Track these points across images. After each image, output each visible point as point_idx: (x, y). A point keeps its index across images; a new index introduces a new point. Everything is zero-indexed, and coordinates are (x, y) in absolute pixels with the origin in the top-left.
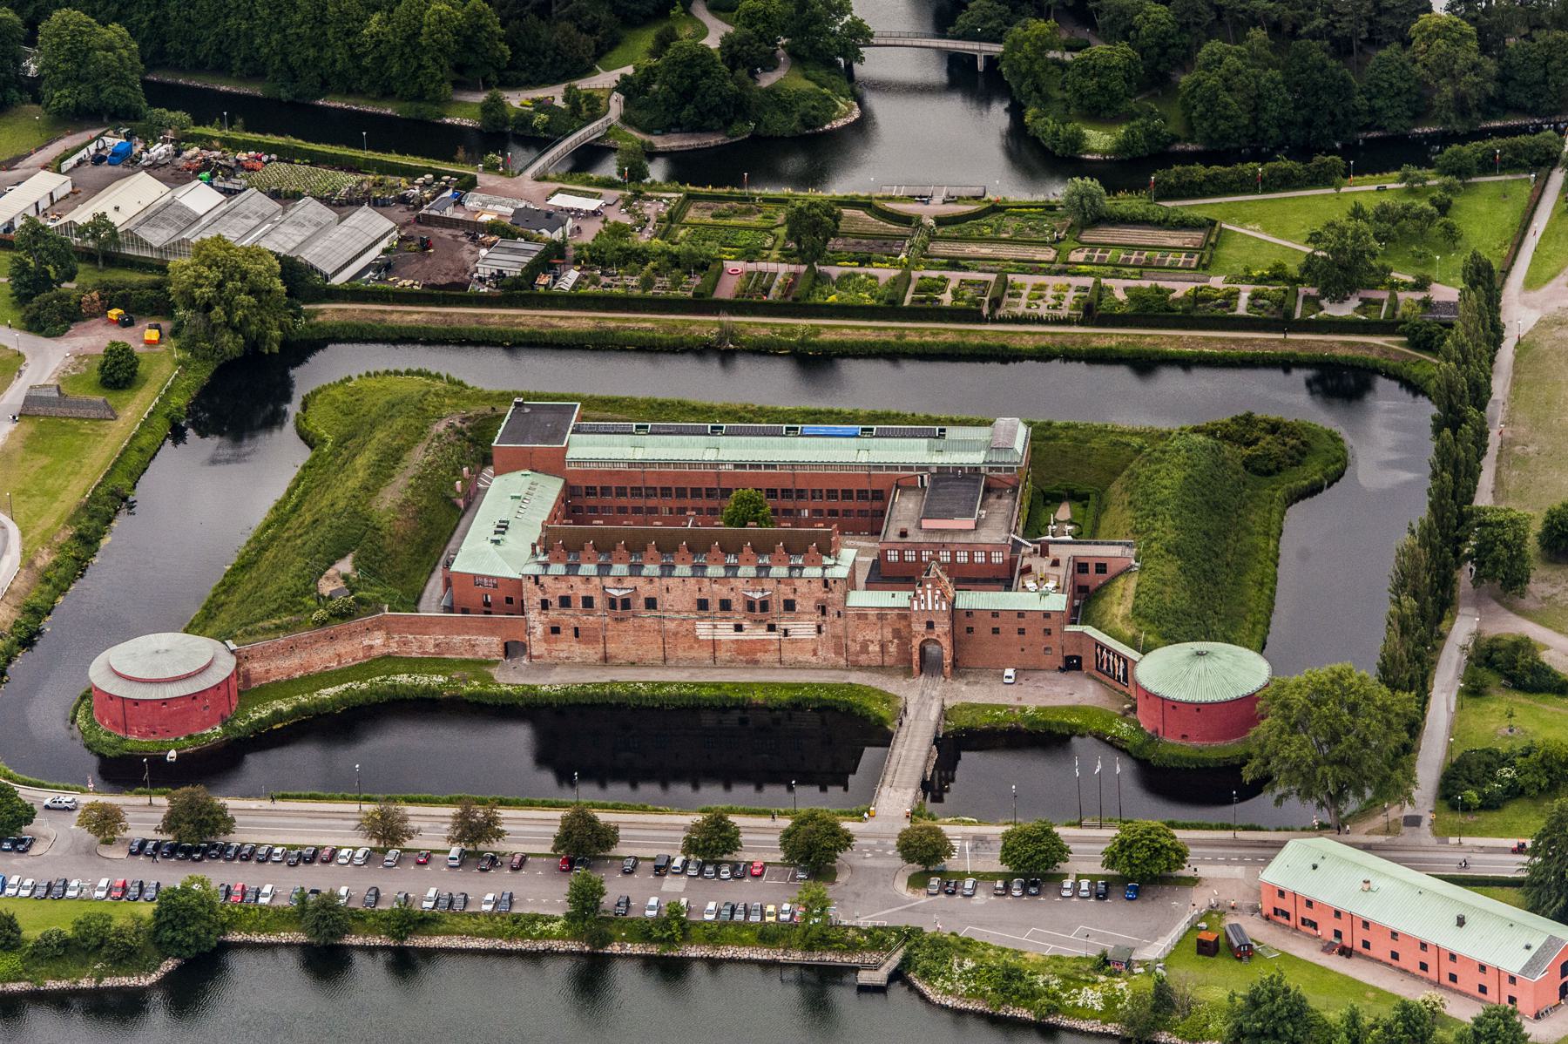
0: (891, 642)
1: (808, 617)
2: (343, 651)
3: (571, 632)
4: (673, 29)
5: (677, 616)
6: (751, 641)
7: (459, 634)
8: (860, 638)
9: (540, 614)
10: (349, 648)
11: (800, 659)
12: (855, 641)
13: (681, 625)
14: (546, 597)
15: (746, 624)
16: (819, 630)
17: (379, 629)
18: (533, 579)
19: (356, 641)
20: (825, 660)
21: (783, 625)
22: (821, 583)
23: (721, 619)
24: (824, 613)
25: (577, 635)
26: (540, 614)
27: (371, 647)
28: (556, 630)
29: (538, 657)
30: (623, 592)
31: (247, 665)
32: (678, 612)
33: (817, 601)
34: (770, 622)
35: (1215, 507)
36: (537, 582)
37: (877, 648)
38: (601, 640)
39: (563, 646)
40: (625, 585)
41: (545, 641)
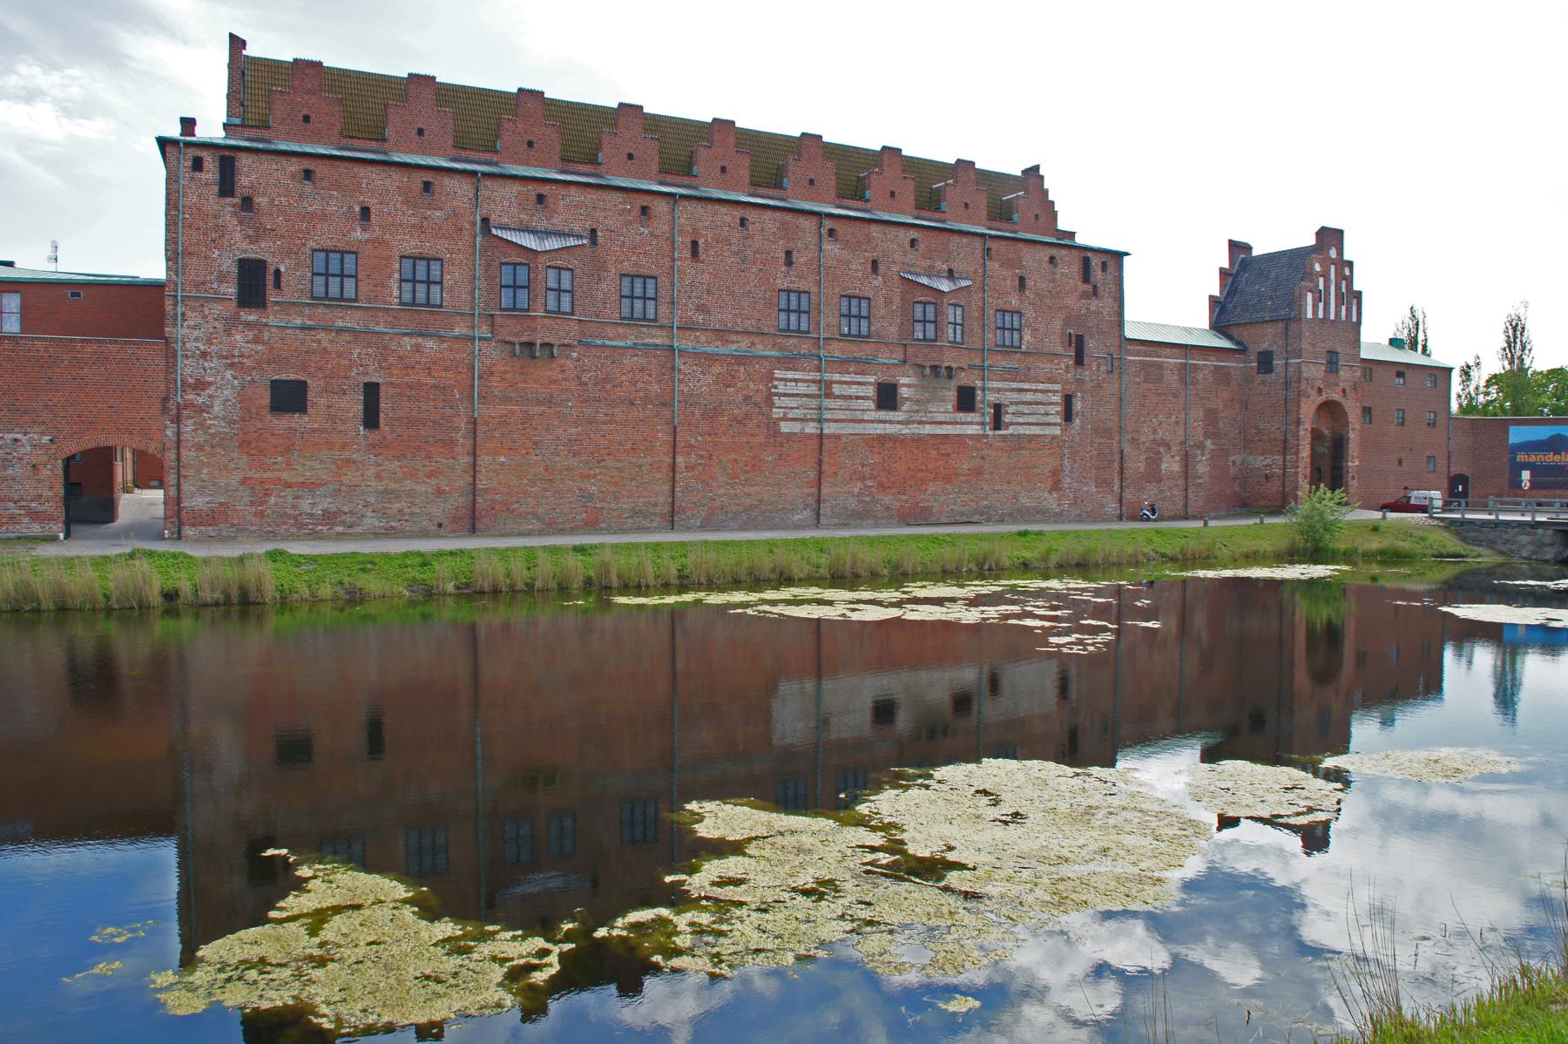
0: (1201, 446)
1: (1046, 367)
4: (181, 135)
6: (917, 440)
8: (1146, 437)
9: (231, 324)
12: (1134, 442)
13: (727, 381)
15: (907, 385)
16: (1068, 415)
18: (211, 172)
21: (992, 391)
22: (1075, 269)
23: (843, 364)
24: (1079, 361)
25: (371, 419)
28: (289, 397)
30: (552, 244)
32: (721, 334)
33: (1067, 322)
34: (964, 379)
35: (980, 565)
36: (227, 186)
37: (1176, 467)
40: (557, 222)
41: (244, 444)
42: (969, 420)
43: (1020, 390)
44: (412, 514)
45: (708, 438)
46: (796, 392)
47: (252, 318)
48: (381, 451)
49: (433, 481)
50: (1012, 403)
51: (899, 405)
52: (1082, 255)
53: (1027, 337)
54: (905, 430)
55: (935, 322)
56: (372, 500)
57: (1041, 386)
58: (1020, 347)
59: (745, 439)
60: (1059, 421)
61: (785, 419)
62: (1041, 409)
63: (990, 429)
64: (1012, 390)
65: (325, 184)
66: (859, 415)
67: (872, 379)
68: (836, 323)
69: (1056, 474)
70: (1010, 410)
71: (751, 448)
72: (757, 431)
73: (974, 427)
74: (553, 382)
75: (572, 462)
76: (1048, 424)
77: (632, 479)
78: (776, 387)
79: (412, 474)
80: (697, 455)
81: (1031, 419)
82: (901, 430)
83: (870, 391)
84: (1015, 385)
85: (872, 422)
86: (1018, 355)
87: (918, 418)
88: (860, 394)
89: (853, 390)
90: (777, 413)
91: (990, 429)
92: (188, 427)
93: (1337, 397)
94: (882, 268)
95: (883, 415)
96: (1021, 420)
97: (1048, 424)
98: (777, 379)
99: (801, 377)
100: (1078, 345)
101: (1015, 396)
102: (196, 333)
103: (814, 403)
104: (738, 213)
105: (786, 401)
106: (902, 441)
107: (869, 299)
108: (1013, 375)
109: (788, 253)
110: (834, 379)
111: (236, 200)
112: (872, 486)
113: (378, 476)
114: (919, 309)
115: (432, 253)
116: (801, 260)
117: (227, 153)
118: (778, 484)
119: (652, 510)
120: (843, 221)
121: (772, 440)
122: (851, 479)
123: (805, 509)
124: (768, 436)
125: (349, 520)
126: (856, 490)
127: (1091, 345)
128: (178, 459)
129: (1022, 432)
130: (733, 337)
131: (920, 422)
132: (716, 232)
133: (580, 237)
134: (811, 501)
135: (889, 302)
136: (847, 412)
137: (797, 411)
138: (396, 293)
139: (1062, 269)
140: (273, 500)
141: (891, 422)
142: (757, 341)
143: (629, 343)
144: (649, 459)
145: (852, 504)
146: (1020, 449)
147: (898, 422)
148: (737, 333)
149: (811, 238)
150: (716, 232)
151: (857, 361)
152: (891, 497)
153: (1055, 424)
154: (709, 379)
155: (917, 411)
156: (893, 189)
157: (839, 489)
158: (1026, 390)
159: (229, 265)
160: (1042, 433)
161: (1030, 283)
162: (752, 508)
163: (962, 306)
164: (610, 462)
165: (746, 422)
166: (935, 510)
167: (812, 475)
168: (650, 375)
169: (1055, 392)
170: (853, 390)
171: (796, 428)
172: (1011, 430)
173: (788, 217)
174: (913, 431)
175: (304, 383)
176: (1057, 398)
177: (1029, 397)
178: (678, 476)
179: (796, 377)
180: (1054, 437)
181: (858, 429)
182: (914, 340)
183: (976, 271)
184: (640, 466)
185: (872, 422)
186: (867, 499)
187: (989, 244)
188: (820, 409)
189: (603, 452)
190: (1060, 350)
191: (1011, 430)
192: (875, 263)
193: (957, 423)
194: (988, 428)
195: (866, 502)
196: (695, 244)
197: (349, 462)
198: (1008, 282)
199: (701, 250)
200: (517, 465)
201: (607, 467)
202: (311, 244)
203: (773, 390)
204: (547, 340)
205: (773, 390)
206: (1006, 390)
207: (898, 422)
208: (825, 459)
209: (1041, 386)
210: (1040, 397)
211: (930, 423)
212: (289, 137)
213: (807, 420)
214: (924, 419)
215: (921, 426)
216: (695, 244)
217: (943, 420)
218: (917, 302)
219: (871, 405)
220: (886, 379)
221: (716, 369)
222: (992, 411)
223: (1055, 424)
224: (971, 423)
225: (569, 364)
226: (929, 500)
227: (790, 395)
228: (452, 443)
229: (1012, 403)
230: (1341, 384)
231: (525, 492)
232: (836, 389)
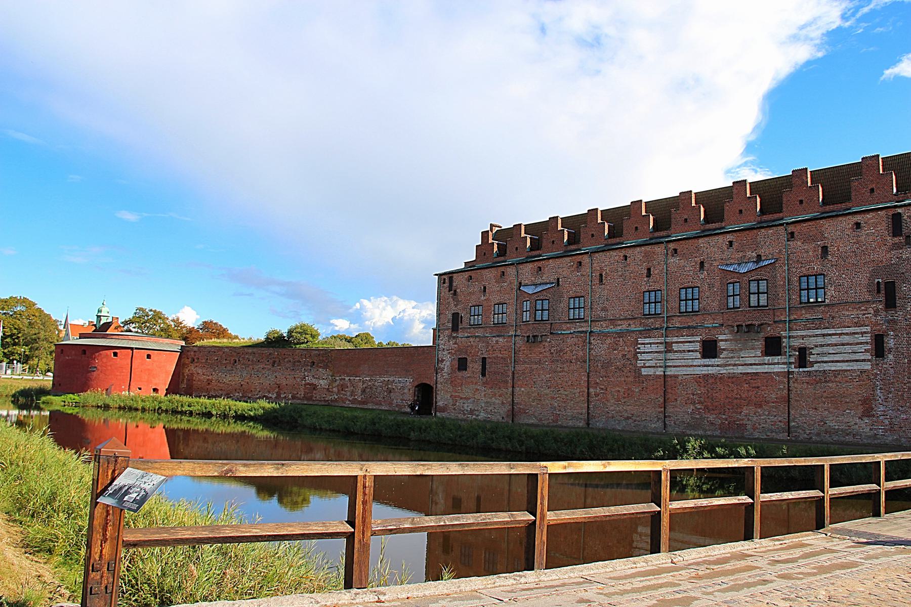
3: (478, 367)
5: (611, 329)
6: (732, 377)
7: (380, 375)
9: (450, 337)
10: (290, 381)
11: (832, 424)
14: (459, 309)
15: (724, 340)
19: (299, 374)
20: (892, 428)
24: (890, 303)
26: (450, 337)
27: (314, 387)
29: (443, 410)
31: (192, 368)
32: (613, 321)
33: (875, 273)
34: (770, 331)
38: (509, 379)
39: (467, 391)
40: (545, 278)
42: (776, 361)
43: (824, 335)
44: (494, 412)
45: (605, 379)
46: (651, 350)
47: (455, 335)
48: (486, 385)
49: (501, 398)
50: (816, 346)
51: (718, 354)
52: (891, 212)
53: (831, 291)
54: (723, 371)
55: (750, 293)
56: (483, 405)
58: (824, 302)
59: (623, 379)
60: (870, 358)
61: (643, 367)
62: (848, 348)
63: (795, 367)
64: (817, 336)
65: (474, 280)
66: (690, 362)
68: (677, 305)
71: (626, 384)
72: (629, 374)
73: (780, 366)
74: (541, 353)
75: (547, 391)
76: (857, 361)
77: (572, 400)
78: (639, 349)
79: (495, 395)
80: (600, 388)
81: (837, 358)
82: (719, 371)
83: (698, 346)
85: (699, 366)
86: (822, 308)
87: (733, 362)
88: (690, 349)
89: (687, 347)
90: (640, 363)
91: (795, 367)
92: (439, 376)
94: (706, 265)
95: (707, 361)
96: (825, 359)
97: (857, 361)
98: (640, 344)
99: (653, 341)
101: (820, 340)
102: (442, 342)
103: (661, 356)
104: (622, 253)
105: (645, 356)
106: (721, 378)
107: (699, 287)
108: (818, 323)
109: (649, 270)
110: (674, 340)
111: (453, 292)
112: (700, 409)
113: (485, 395)
114: (731, 287)
115: (504, 302)
116: (656, 272)
117: (451, 275)
118: (642, 405)
119: (580, 416)
120: (681, 242)
121: (637, 379)
122: (686, 403)
123: (658, 421)
124: (635, 378)
125: (477, 413)
126: (690, 411)
128: (436, 388)
129: (826, 369)
130: (619, 322)
131: (735, 365)
132: (611, 267)
133: (553, 283)
134: (662, 416)
135: (711, 286)
136: (683, 361)
137: (651, 361)
138: (492, 320)
139: (863, 232)
140: (458, 404)
141: (713, 366)
143: (572, 331)
144: (578, 390)
145: (687, 418)
146: (826, 382)
147: (718, 366)
148: (621, 320)
149: (662, 258)
150: (611, 267)
151: (689, 327)
152: (714, 416)
153: (864, 360)
154: (605, 346)
155: (732, 357)
156: (741, 208)
157: (678, 410)
158: (830, 335)
159: (450, 317)
160: (848, 368)
162: (628, 418)
163: (766, 280)
164: (562, 391)
165: (624, 369)
166: (749, 427)
167: (662, 400)
168: (578, 347)
169: (862, 333)
170: (687, 347)
171: (651, 372)
172: (816, 367)
173: (648, 248)
174: (729, 371)
175: (466, 358)
176: (867, 338)
177: (834, 340)
178: (591, 399)
179: (651, 341)
180: (862, 372)
181: (690, 371)
182: (728, 309)
183: (780, 251)
184: (574, 394)
185: (699, 366)
186: (698, 416)
187: (791, 229)
189: (559, 386)
190: (868, 297)
191: (816, 367)
192: (702, 264)
193: (766, 364)
194: (793, 366)
195: (697, 418)
196: (601, 275)
197: (477, 390)
198: (811, 253)
199: (604, 278)
200: (528, 392)
201: (560, 394)
202: (470, 304)
203: (638, 350)
204: (535, 334)
205: (638, 350)
206: (810, 336)
207: (718, 366)
210: (846, 339)
211: (742, 365)
212: (792, 214)
213: (657, 367)
214: (737, 362)
215: (735, 367)
216: (601, 275)
218: (729, 283)
219: (699, 356)
221: (608, 341)
222: (797, 353)
223: (864, 360)
224: (778, 363)
225: (547, 344)
226: (743, 420)
227: (647, 353)
228: (507, 382)
229: (816, 346)
231: (531, 405)
232: (675, 347)
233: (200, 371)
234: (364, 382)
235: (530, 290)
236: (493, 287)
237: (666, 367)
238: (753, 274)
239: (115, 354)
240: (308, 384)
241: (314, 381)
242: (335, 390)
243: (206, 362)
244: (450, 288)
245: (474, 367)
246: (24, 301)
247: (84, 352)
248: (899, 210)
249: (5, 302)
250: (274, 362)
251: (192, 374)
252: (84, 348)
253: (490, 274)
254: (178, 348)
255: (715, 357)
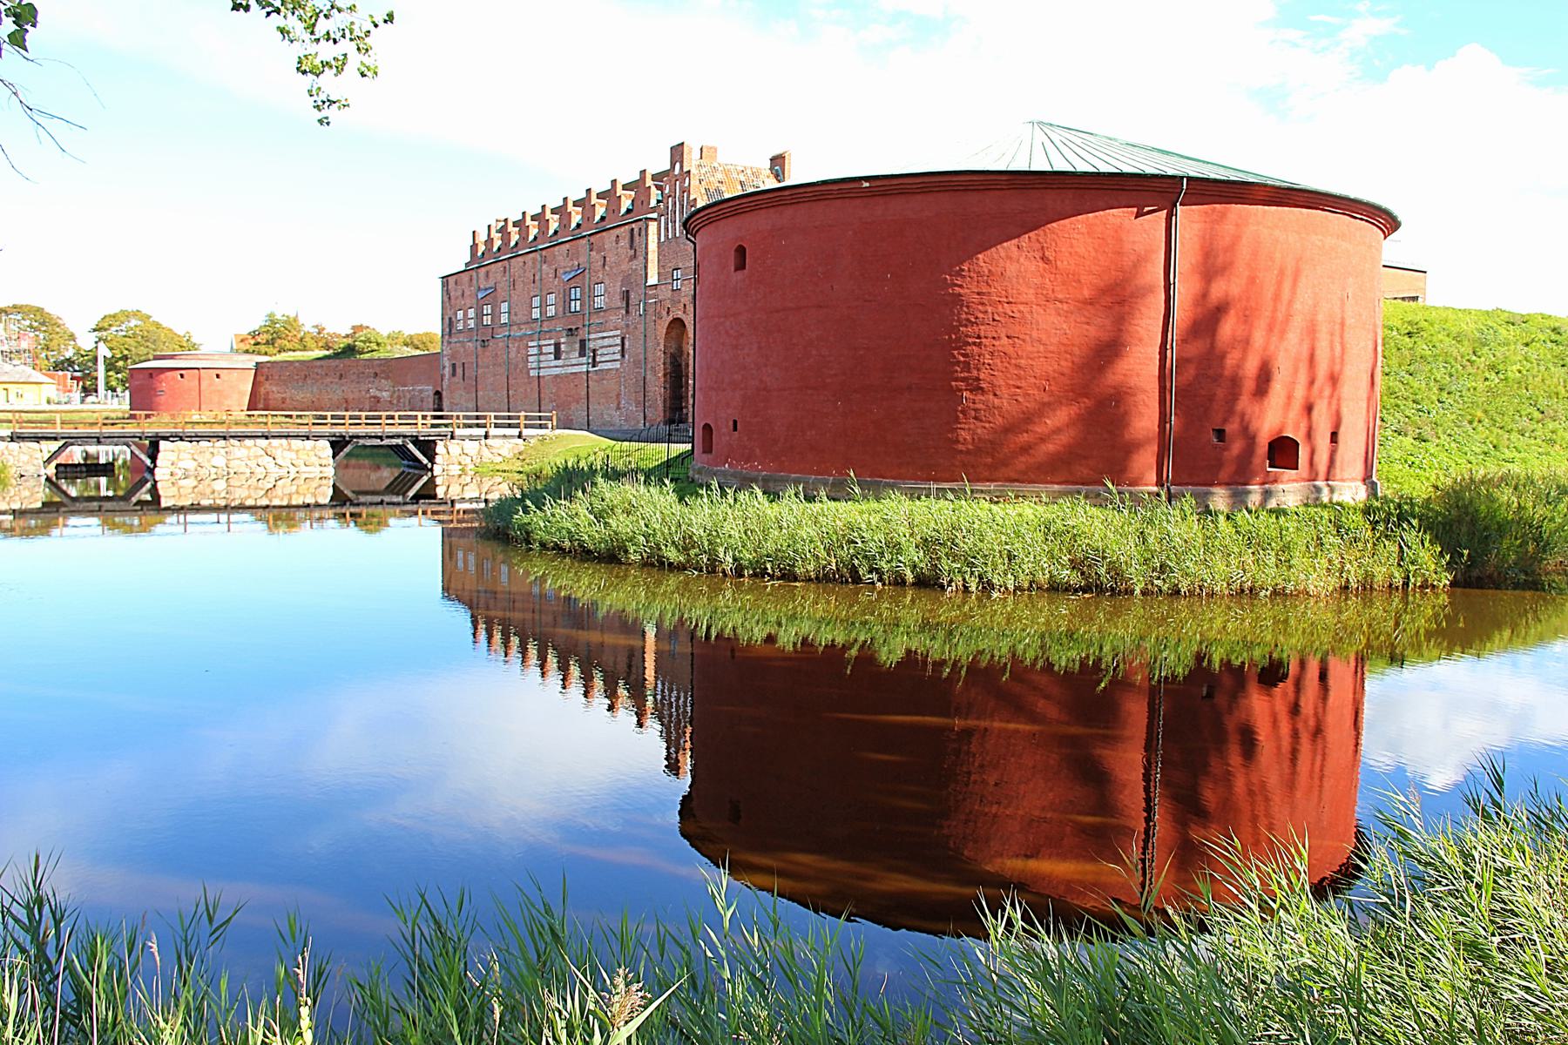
2: (351, 396)
6: (567, 376)
10: (357, 395)
16: (623, 356)
17: (387, 378)
19: (364, 387)
24: (627, 312)
26: (449, 343)
27: (378, 400)
34: (583, 334)
57: (611, 333)
62: (611, 350)
67: (552, 342)
69: (618, 395)
70: (599, 352)
75: (491, 394)
81: (607, 358)
83: (552, 349)
84: (601, 335)
86: (602, 314)
93: (680, 314)
96: (603, 359)
100: (626, 296)
108: (602, 327)
127: (632, 296)
130: (522, 327)
142: (526, 326)
151: (550, 331)
161: (607, 259)
176: (618, 341)
177: (606, 342)
180: (617, 370)
188: (539, 361)
208: (542, 391)
209: (611, 333)
210: (611, 341)
217: (576, 364)
219: (552, 356)
220: (557, 341)
230: (682, 300)
232: (545, 350)
233: (274, 389)
234: (409, 391)
235: (480, 296)
236: (467, 293)
237: (540, 368)
238: (573, 281)
239: (182, 376)
240: (374, 397)
241: (378, 394)
242: (395, 402)
243: (279, 379)
244: (448, 293)
245: (459, 371)
246: (137, 314)
247: (151, 375)
248: (633, 225)
249: (114, 317)
250: (341, 375)
251: (268, 393)
252: (150, 371)
253: (465, 277)
254: (252, 365)
255: (559, 359)
